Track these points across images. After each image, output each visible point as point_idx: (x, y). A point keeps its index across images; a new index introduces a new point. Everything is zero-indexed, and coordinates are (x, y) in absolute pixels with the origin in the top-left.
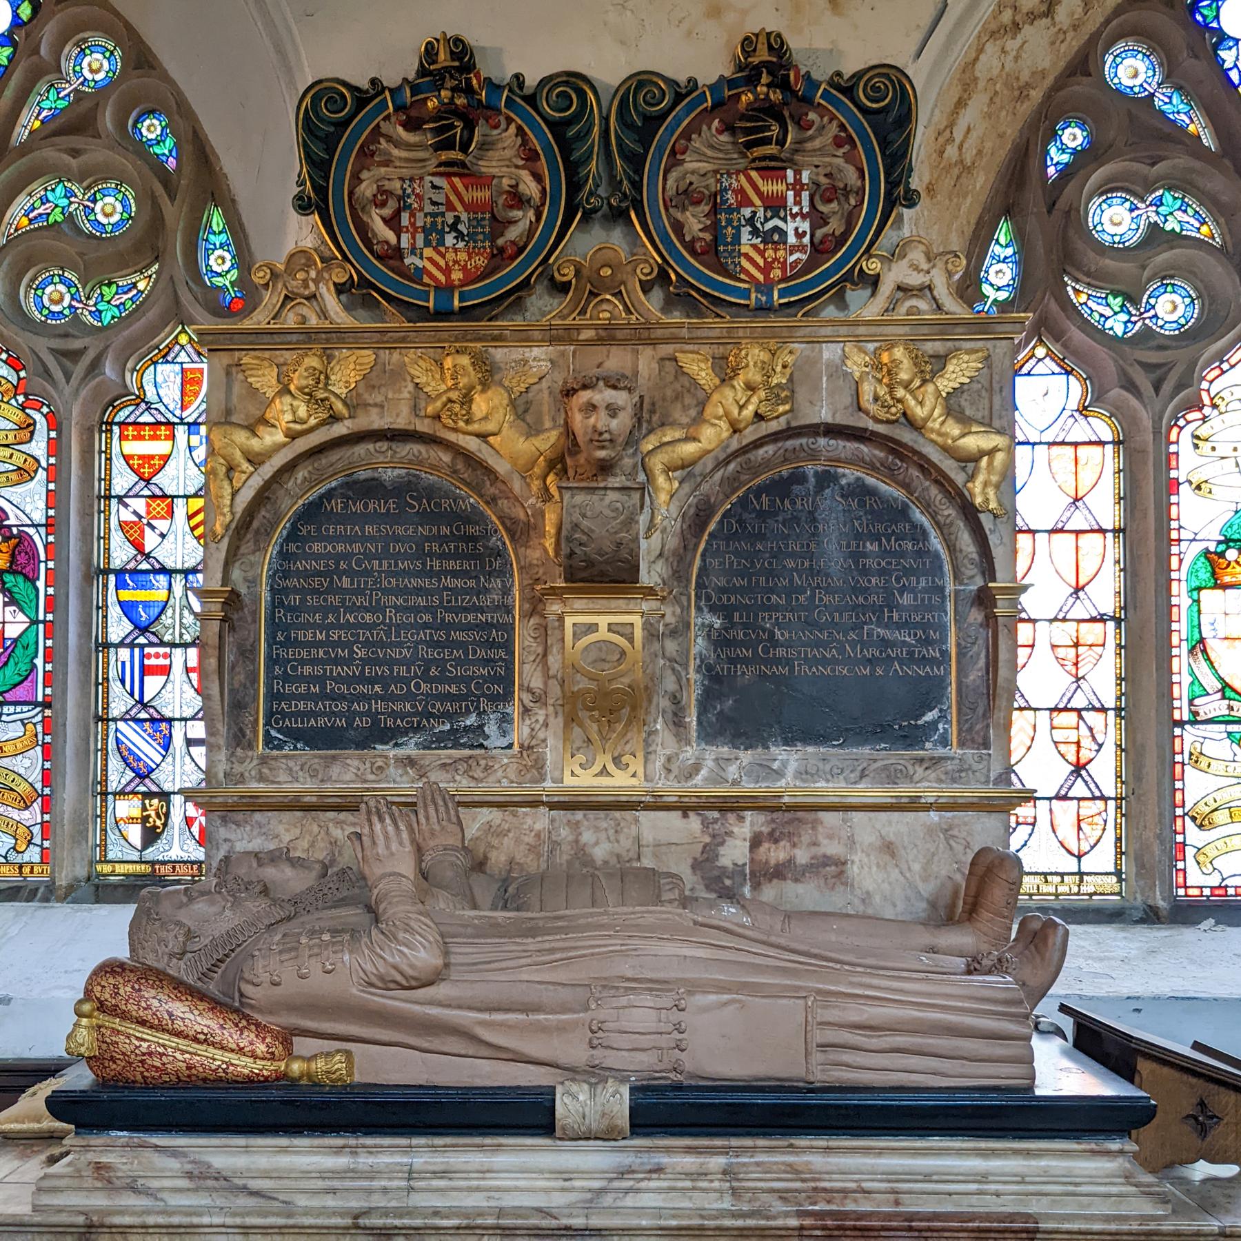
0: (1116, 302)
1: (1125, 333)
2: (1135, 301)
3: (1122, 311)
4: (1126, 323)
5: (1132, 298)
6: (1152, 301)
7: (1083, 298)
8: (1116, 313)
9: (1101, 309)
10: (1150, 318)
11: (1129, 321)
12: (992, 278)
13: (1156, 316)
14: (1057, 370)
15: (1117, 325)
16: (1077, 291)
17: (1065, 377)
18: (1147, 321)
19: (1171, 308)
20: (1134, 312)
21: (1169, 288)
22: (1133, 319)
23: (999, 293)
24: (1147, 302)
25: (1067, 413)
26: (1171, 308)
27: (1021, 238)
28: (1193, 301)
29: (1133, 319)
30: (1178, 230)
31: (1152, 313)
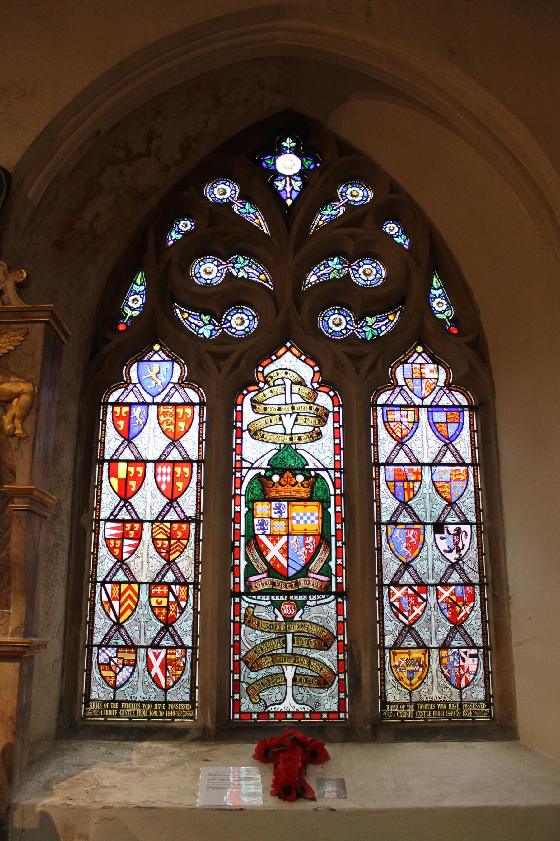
0: (206, 318)
1: (211, 336)
2: (219, 320)
3: (210, 324)
4: (211, 331)
5: (217, 316)
6: (229, 318)
7: (186, 315)
8: (206, 325)
9: (196, 322)
10: (227, 328)
11: (214, 329)
12: (130, 303)
13: (231, 327)
14: (166, 358)
15: (206, 332)
16: (182, 312)
17: (171, 363)
18: (225, 330)
19: (241, 322)
20: (217, 324)
21: (240, 311)
22: (216, 328)
23: (134, 312)
24: (226, 318)
25: (171, 385)
26: (241, 322)
27: (148, 279)
28: (254, 318)
29: (216, 328)
30: (246, 276)
31: (229, 324)
